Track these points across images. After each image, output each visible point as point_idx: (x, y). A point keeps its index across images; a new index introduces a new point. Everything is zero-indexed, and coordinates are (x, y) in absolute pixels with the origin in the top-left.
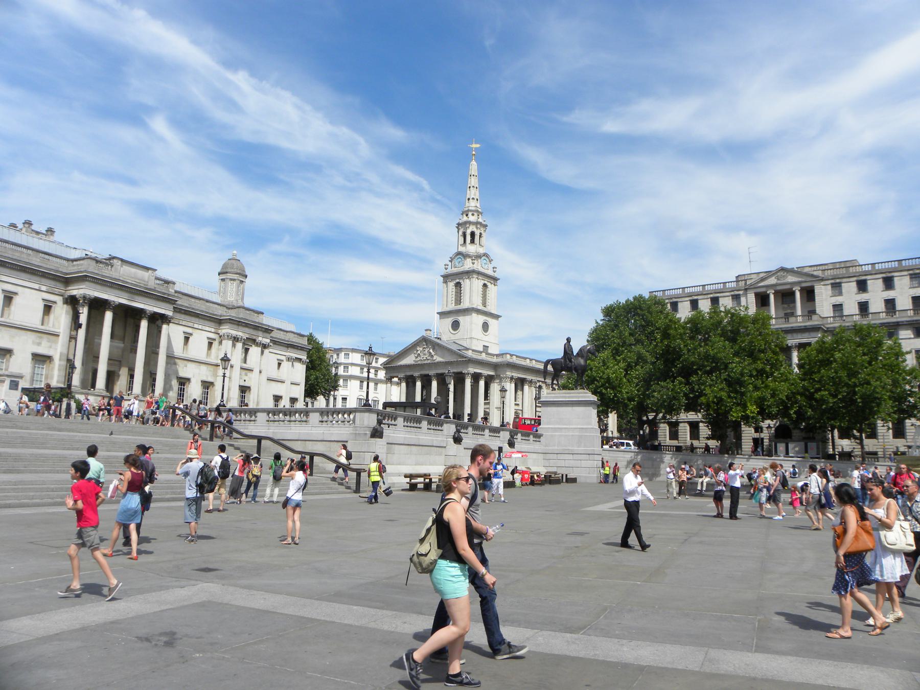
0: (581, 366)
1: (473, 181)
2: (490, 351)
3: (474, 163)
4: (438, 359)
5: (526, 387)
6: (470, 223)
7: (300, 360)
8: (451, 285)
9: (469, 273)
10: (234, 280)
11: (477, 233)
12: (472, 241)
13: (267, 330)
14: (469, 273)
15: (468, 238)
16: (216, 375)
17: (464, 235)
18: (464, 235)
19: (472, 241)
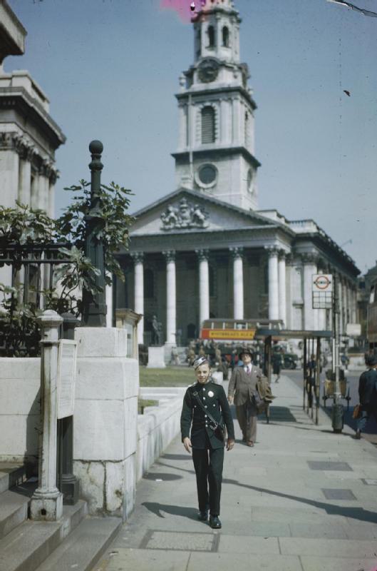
4: (211, 225)
6: (221, 11)
8: (195, 111)
11: (231, 28)
12: (225, 44)
15: (219, 36)
18: (211, 32)
19: (225, 44)
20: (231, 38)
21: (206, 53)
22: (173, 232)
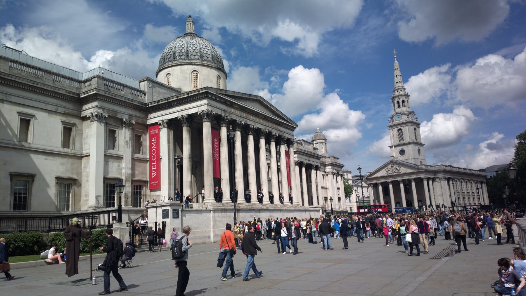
1: (397, 72)
2: (423, 164)
3: (396, 62)
5: (451, 182)
6: (401, 95)
11: (406, 100)
16: (327, 194)
17: (398, 102)
21: (398, 110)
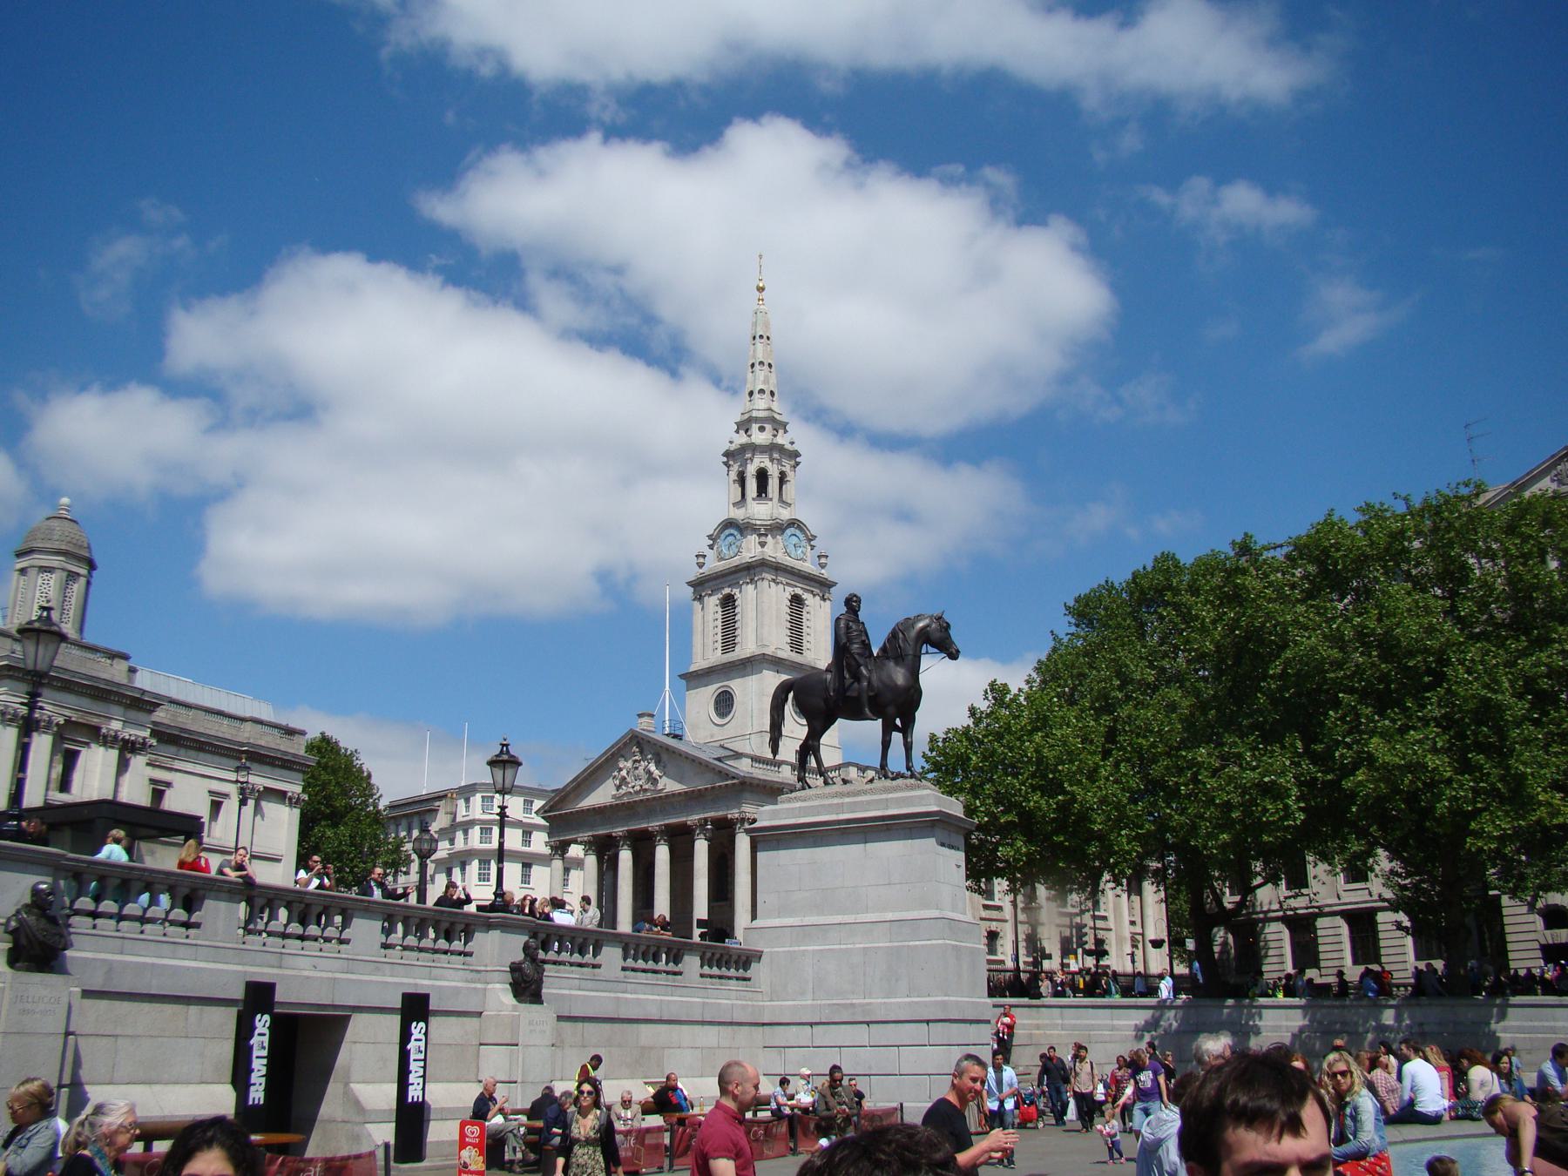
0: (894, 688)
4: (669, 785)
6: (754, 448)
7: (280, 796)
8: (713, 602)
9: (751, 570)
10: (50, 570)
11: (773, 471)
13: (142, 704)
14: (751, 570)
15: (752, 485)
17: (742, 480)
18: (742, 480)
20: (773, 484)
22: (626, 800)
